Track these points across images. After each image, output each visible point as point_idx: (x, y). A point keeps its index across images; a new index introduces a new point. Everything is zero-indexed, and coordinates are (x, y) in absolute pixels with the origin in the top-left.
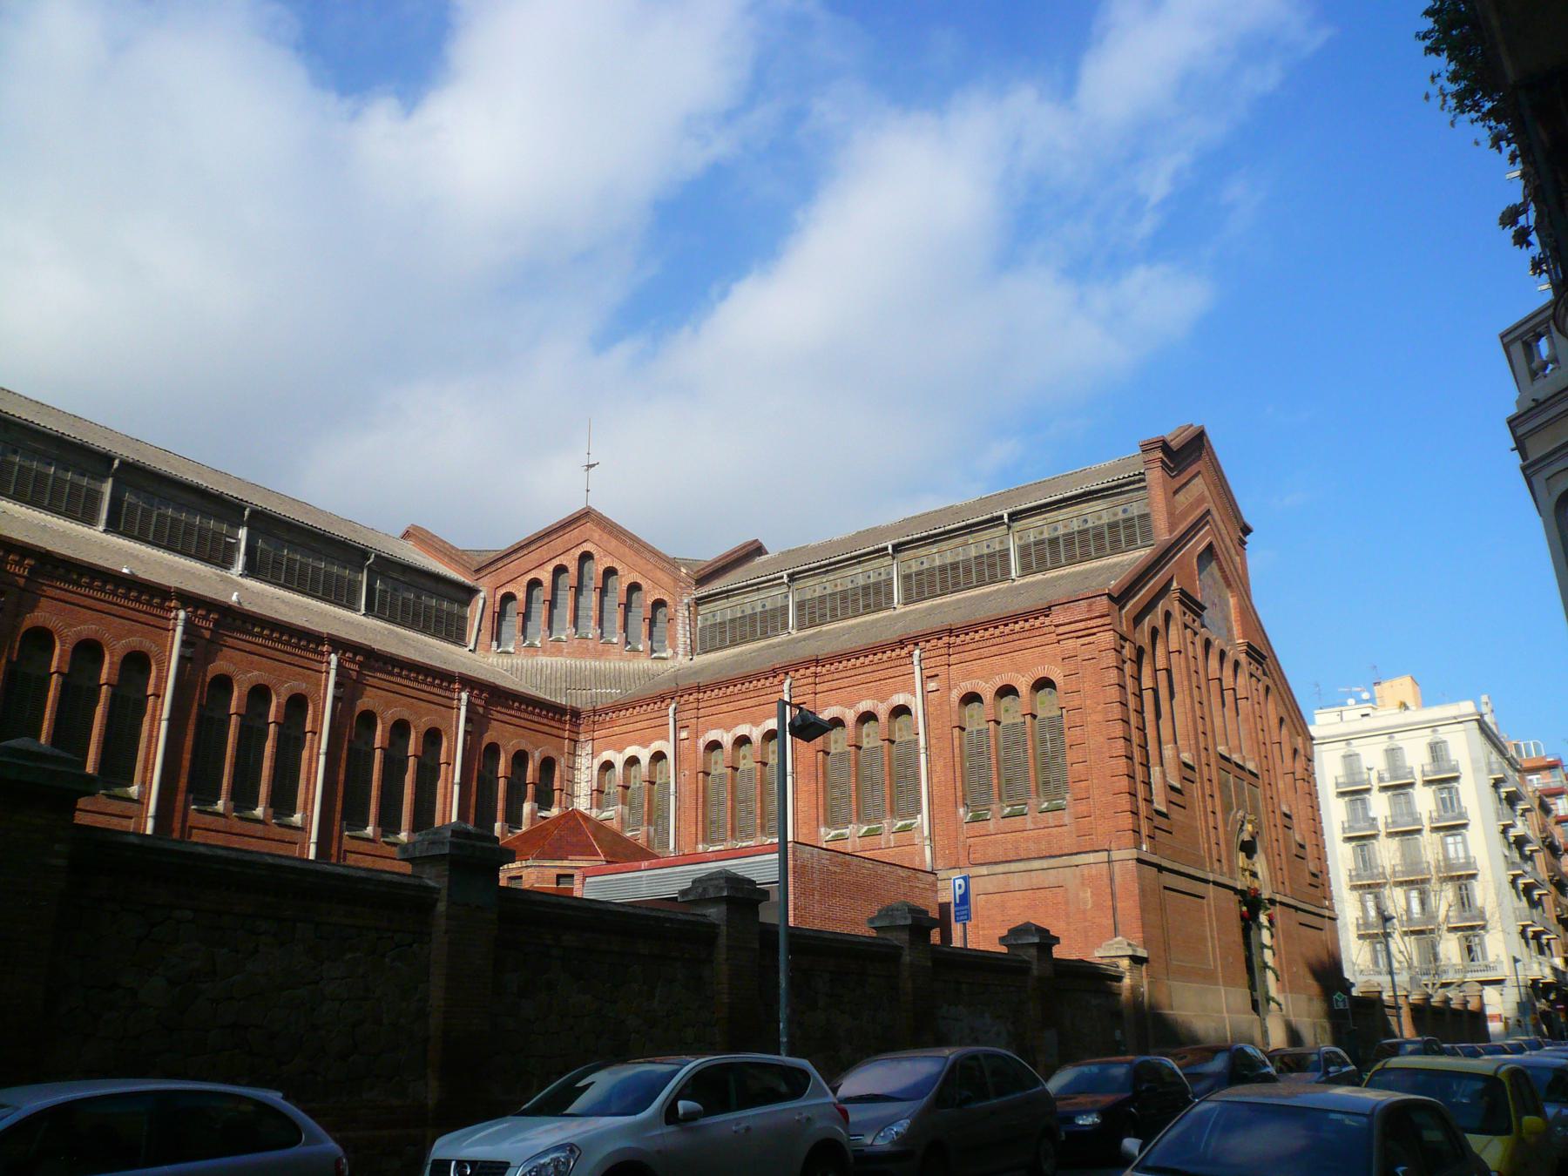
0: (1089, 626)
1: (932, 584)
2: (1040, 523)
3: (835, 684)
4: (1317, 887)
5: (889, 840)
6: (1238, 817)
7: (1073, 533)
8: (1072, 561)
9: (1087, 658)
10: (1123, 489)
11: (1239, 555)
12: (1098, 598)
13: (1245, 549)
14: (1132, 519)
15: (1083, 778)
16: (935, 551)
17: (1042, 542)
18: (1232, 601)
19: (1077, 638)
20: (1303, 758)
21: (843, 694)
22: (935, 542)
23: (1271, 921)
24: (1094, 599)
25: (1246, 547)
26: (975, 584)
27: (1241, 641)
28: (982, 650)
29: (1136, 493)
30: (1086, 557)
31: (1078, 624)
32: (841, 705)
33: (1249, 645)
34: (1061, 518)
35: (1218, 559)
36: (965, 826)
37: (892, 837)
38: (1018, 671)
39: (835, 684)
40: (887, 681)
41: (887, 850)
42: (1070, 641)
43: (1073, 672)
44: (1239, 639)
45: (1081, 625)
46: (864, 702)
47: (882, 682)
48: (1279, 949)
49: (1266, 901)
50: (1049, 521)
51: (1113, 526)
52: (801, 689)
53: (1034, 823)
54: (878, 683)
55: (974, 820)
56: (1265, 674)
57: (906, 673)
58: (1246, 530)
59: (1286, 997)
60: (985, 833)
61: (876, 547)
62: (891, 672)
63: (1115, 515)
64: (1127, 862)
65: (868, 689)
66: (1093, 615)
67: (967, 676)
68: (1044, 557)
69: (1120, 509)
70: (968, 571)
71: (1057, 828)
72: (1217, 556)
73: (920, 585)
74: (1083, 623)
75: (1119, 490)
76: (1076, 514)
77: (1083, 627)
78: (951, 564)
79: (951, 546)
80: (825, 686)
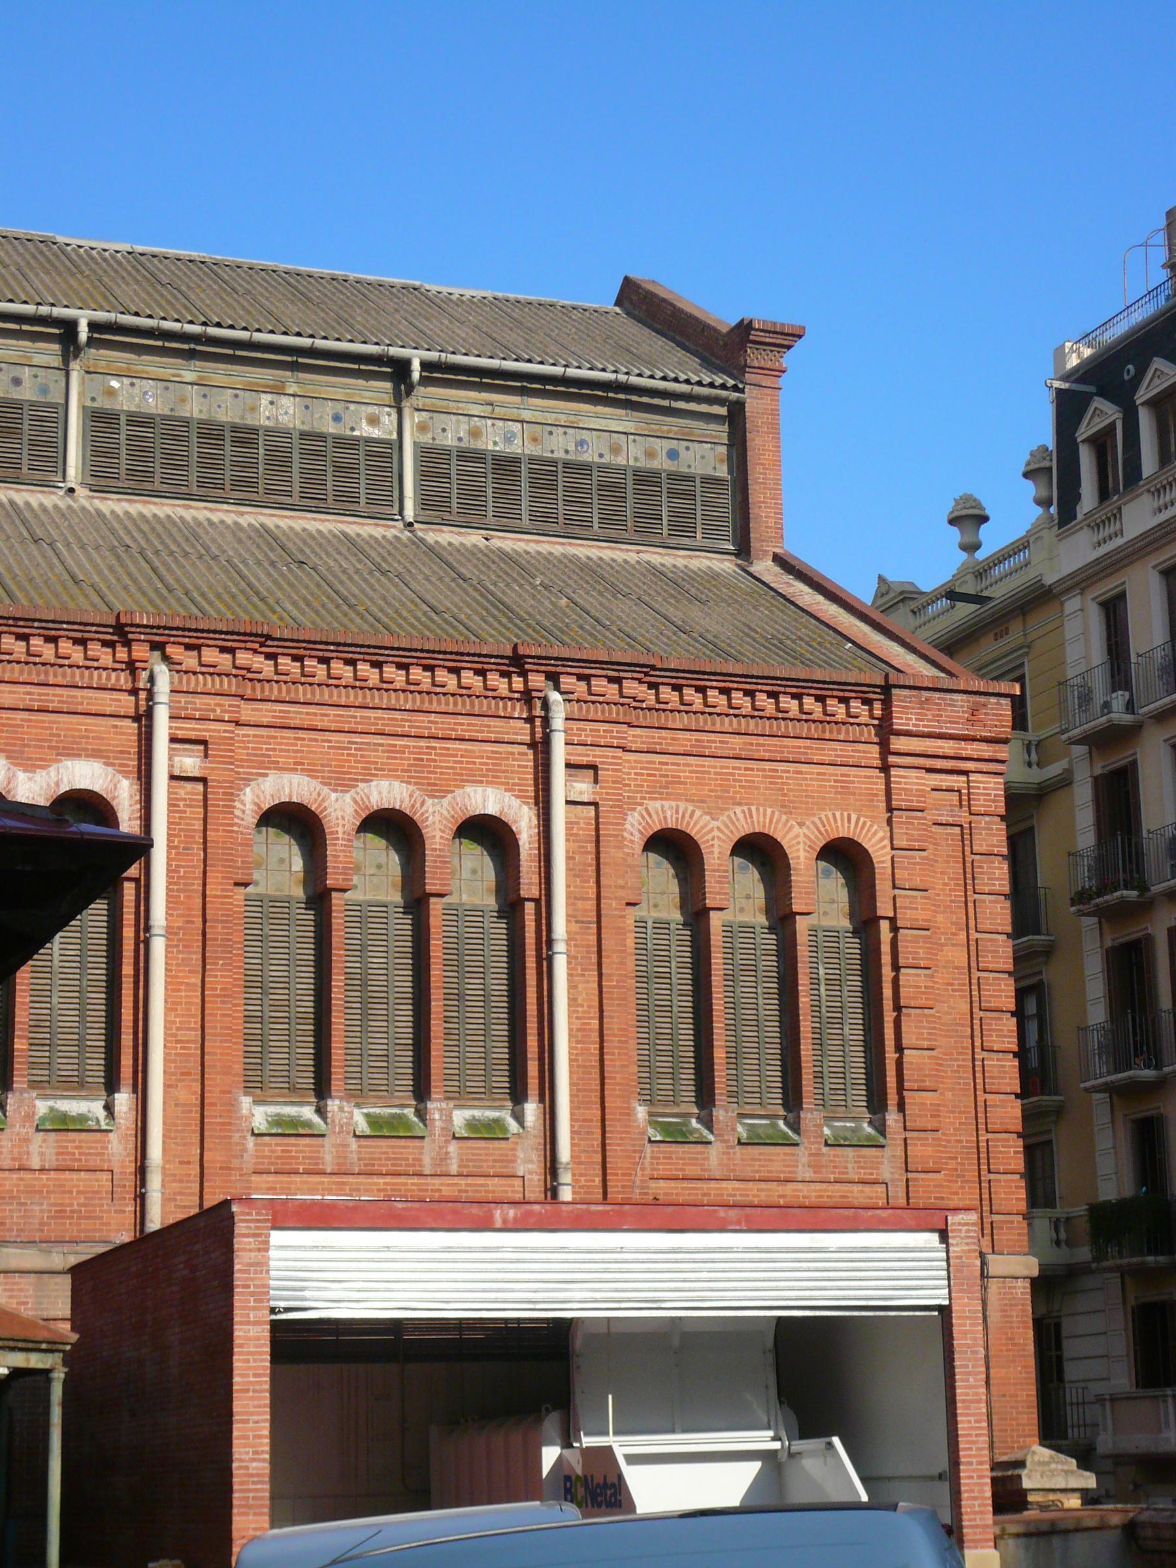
0: (964, 753)
1: (175, 462)
2: (475, 410)
3: (298, 715)
5: (445, 1157)
7: (554, 463)
8: (544, 523)
9: (943, 819)
10: (635, 398)
12: (993, 700)
14: (689, 478)
15: (927, 1084)
16: (189, 376)
17: (477, 456)
19: (930, 770)
21: (319, 745)
22: (191, 355)
24: (982, 699)
26: (295, 499)
28: (704, 737)
29: (701, 425)
30: (575, 529)
31: (940, 742)
32: (311, 773)
34: (526, 415)
36: (648, 1148)
37: (453, 1147)
38: (787, 808)
39: (298, 715)
40: (448, 744)
41: (437, 1181)
42: (913, 773)
43: (916, 845)
45: (948, 747)
46: (384, 784)
47: (434, 743)
50: (499, 411)
51: (646, 479)
52: (199, 701)
53: (816, 1167)
54: (422, 743)
55: (677, 1136)
57: (506, 737)
60: (691, 1171)
61: (44, 310)
62: (462, 727)
63: (650, 454)
64: (1014, 1283)
65: (392, 750)
66: (978, 734)
67: (664, 788)
68: (479, 494)
69: (662, 447)
70: (279, 460)
71: (860, 1187)
73: (140, 451)
74: (951, 743)
75: (665, 403)
76: (563, 419)
77: (951, 752)
78: (235, 428)
79: (238, 382)
80: (266, 713)
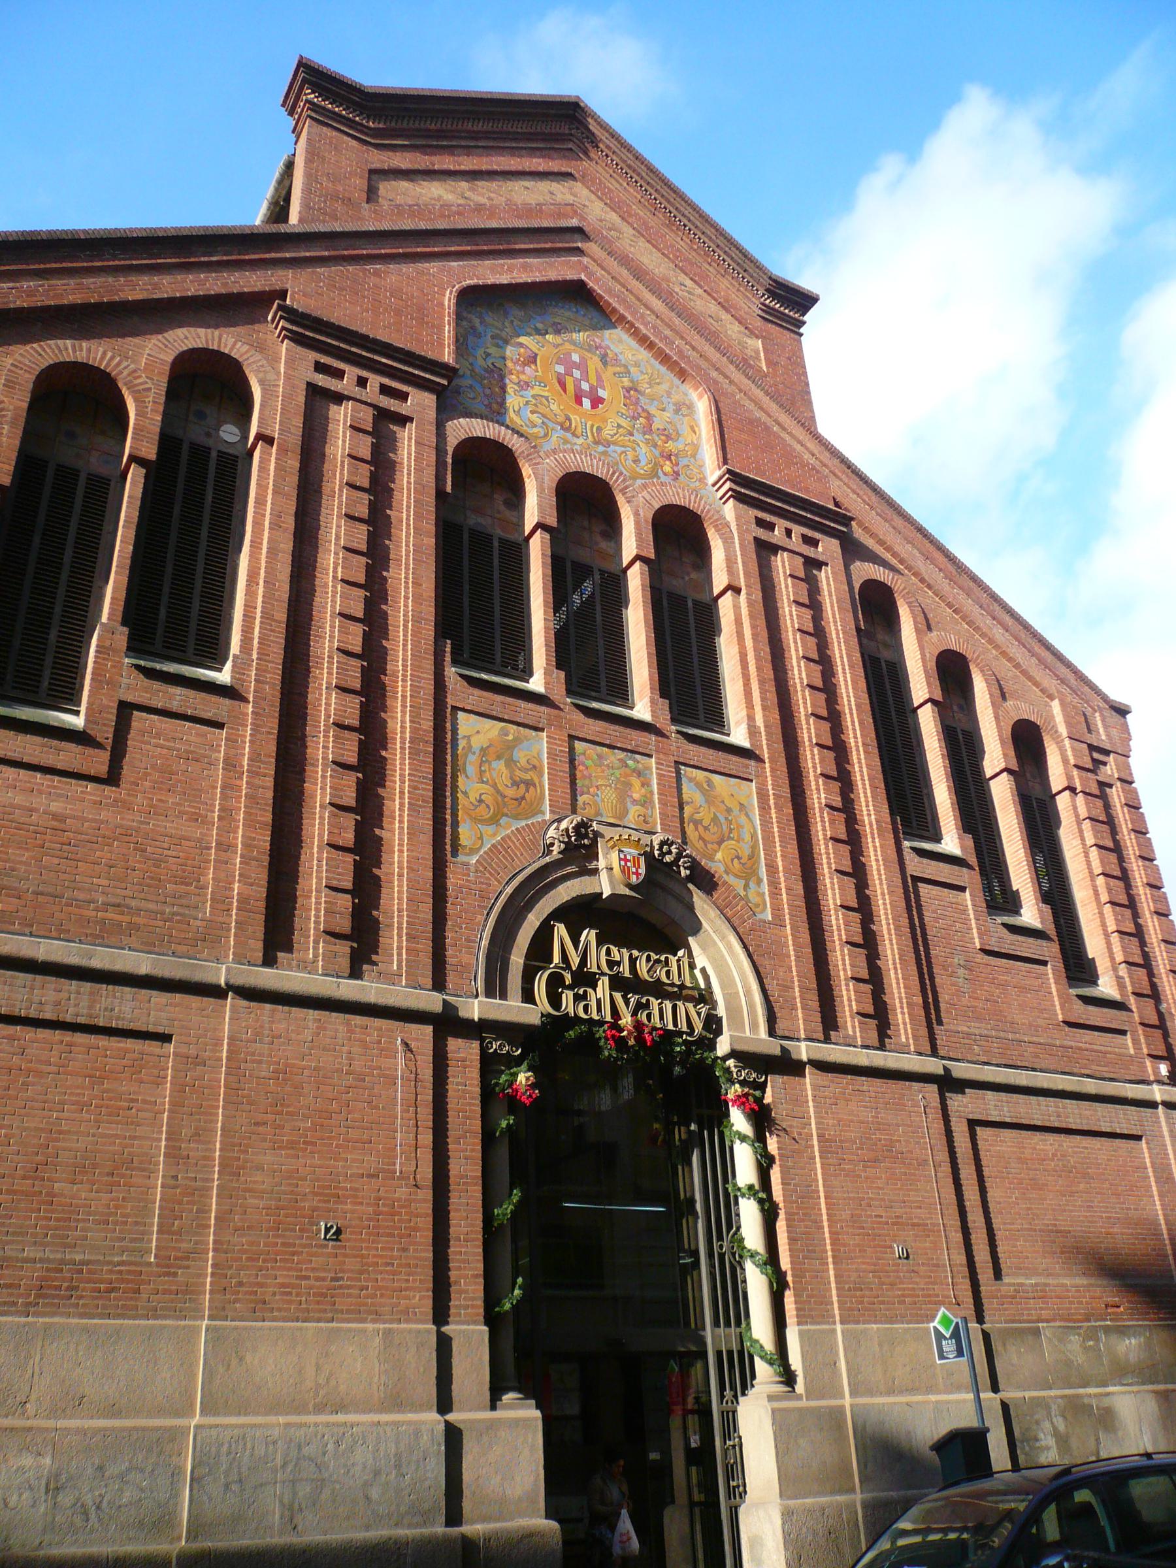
4: (1123, 1032)
6: (551, 832)
11: (757, 337)
13: (801, 335)
18: (702, 406)
20: (1067, 742)
23: (762, 1119)
25: (802, 330)
27: (718, 473)
33: (734, 476)
35: (622, 318)
44: (712, 473)
48: (803, 1196)
49: (731, 1063)
56: (852, 550)
58: (803, 301)
59: (812, 1344)
72: (614, 310)
